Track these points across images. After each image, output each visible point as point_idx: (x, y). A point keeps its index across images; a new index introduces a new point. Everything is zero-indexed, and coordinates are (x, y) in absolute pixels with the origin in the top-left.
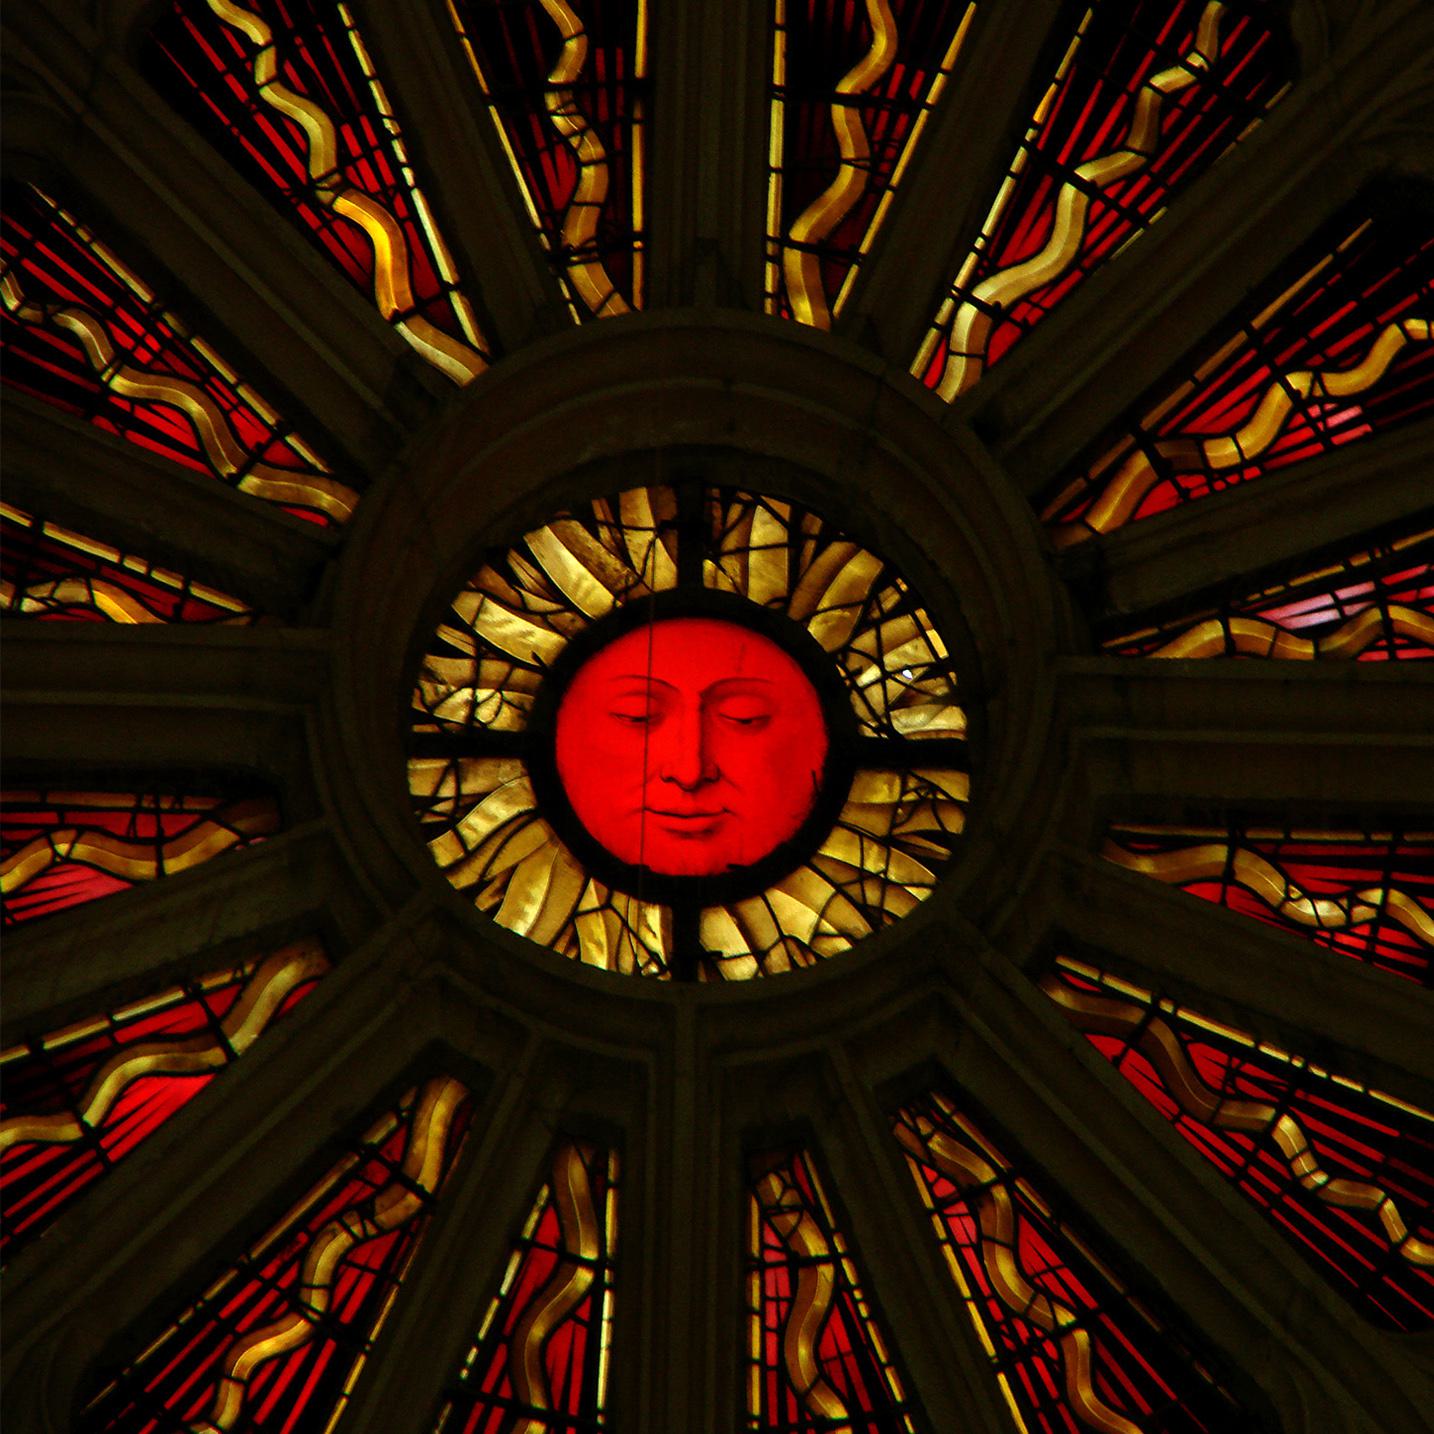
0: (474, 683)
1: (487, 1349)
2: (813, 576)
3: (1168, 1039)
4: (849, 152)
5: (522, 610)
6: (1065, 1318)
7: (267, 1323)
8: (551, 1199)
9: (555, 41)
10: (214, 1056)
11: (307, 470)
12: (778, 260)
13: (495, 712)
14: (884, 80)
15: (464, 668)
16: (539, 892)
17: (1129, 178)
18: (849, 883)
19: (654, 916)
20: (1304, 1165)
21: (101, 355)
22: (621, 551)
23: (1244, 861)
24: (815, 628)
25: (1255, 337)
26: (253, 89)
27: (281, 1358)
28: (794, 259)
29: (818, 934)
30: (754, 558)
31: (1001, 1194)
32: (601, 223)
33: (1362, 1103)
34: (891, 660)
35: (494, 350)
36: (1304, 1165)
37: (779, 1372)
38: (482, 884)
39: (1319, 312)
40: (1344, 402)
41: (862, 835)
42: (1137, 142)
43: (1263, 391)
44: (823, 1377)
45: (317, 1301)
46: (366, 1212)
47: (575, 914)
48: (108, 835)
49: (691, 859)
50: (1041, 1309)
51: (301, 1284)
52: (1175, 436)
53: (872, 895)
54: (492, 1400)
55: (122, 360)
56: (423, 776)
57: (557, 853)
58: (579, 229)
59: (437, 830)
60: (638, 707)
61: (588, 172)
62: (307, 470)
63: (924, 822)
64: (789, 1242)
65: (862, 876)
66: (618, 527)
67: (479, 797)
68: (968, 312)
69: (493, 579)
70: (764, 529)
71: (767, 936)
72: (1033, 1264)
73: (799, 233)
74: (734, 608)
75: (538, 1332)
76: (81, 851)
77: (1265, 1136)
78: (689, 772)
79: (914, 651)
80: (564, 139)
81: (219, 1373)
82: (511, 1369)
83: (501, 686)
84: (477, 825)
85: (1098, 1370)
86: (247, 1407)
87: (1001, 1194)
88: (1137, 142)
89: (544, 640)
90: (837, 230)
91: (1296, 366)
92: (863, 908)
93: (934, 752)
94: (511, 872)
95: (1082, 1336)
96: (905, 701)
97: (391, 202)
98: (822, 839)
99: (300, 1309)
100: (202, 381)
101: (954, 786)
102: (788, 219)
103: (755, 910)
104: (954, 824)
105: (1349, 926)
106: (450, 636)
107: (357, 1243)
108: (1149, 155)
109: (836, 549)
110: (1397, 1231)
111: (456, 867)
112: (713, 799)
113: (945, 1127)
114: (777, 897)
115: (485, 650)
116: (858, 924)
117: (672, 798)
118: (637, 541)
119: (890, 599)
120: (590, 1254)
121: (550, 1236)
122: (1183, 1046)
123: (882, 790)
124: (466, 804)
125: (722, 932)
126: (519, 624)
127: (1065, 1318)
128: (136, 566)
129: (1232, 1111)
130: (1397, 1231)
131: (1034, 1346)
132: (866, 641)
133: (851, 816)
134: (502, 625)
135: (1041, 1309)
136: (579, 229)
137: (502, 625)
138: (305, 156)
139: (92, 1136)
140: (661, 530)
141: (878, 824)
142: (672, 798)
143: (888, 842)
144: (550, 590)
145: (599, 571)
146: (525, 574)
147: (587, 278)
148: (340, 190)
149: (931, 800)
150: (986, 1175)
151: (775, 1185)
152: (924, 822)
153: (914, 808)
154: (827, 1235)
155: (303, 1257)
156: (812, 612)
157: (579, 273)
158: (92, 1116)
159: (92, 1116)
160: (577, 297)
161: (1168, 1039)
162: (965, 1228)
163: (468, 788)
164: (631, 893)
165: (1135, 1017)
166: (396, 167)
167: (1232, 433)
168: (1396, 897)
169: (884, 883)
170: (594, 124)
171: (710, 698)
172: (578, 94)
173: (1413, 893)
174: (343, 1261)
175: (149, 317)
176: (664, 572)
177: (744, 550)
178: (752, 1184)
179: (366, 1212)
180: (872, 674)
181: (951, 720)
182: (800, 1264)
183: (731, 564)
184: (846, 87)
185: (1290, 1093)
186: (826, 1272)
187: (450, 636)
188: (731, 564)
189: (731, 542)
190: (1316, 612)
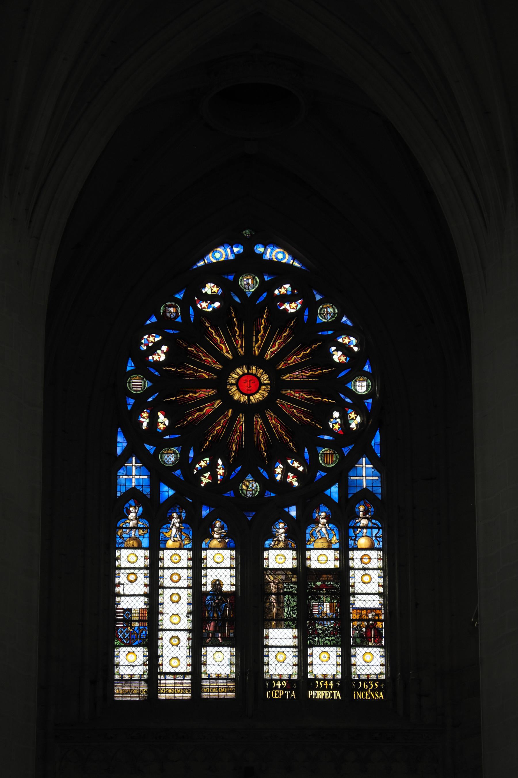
0: (232, 380)
1: (235, 428)
2: (258, 371)
3: (286, 405)
4: (260, 340)
5: (235, 374)
6: (278, 424)
7: (218, 426)
8: (239, 417)
9: (236, 332)
10: (213, 407)
11: (218, 364)
12: (254, 348)
13: (234, 382)
14: (262, 334)
15: (231, 379)
16: (237, 395)
17: (282, 342)
18: (261, 394)
19: (246, 397)
20: (296, 413)
21: (202, 356)
22: (243, 370)
23: (291, 391)
24: (258, 375)
25: (292, 353)
26: (213, 336)
27: (219, 429)
28: (256, 348)
29: (259, 398)
30: (253, 370)
31: (273, 416)
32: (241, 345)
33: (300, 409)
34: (264, 377)
35: (233, 356)
36: (296, 413)
37: (257, 429)
38: (233, 395)
39: (297, 351)
40: (299, 358)
41: (262, 390)
42: (282, 339)
43: (292, 357)
44: (260, 429)
45: (222, 425)
46: (225, 418)
47: (240, 397)
48: (204, 391)
49: (249, 392)
50: (276, 424)
51: (220, 423)
52: (286, 361)
53: (263, 395)
54: (235, 432)
55: (204, 356)
56: (228, 387)
57: (239, 392)
58: (239, 346)
59: (229, 391)
60: (245, 381)
61: (239, 342)
62: (218, 364)
63: (267, 389)
64: (257, 420)
65: (262, 393)
66: (243, 368)
67: (232, 388)
68: (269, 352)
69: (233, 372)
70: (254, 368)
71: (255, 398)
72: (276, 421)
73: (256, 346)
74: (252, 374)
75: (238, 426)
76: (202, 393)
77: (293, 411)
78: (249, 386)
79: (266, 377)
80: (237, 339)
81: (215, 430)
82: (236, 429)
83: (234, 380)
84: (232, 390)
85: (281, 428)
86: (217, 432)
87: (273, 416)
88: (282, 339)
89: (237, 377)
90: (259, 346)
91: (295, 355)
92: (262, 396)
93: (267, 384)
94: (235, 394)
95: (279, 426)
96: (265, 380)
97: (224, 344)
98: (259, 391)
99: (221, 425)
100: (210, 358)
101: (269, 387)
102: (255, 345)
103: (254, 396)
104: (269, 389)
105: (299, 396)
106: (230, 376)
107: (225, 420)
108: (283, 340)
109: (259, 369)
110: (303, 418)
111: (231, 393)
112: (250, 388)
113: (269, 411)
114: (256, 395)
115: (233, 377)
116: (262, 397)
117: (247, 388)
118: (244, 369)
119: (264, 373)
120: (242, 421)
121: (239, 420)
122: (287, 405)
123: (263, 387)
124: (232, 389)
125: (251, 398)
126: (235, 375)
127: (278, 424)
128: (206, 372)
129: (291, 410)
130: (303, 418)
131: (276, 427)
132: (262, 376)
133: (261, 389)
134: (234, 375)
135: (276, 424)
136: (239, 346)
137: (234, 375)
138: (217, 341)
139: (204, 413)
140: (246, 368)
141: (263, 390)
142: (247, 388)
143: (264, 391)
144: (238, 373)
145: (241, 371)
146: (235, 372)
147: (240, 350)
148: (220, 343)
149: (267, 388)
150: (272, 414)
151: (256, 416)
152: (267, 389)
153: (266, 388)
154: (260, 419)
155: (221, 421)
156: (258, 374)
157: (239, 349)
158: (204, 412)
159: (204, 412)
160: (239, 351)
161: (286, 405)
162: (270, 418)
163: (232, 387)
164: (245, 395)
165: (283, 403)
166: (224, 342)
167: (290, 360)
168: (303, 394)
169: (264, 394)
170: (240, 338)
171: (250, 381)
172: (238, 336)
173: (304, 394)
174: (223, 422)
175: (206, 353)
176: (246, 371)
177: (252, 370)
178: (254, 416)
179: (225, 418)
180: (262, 379)
181: (269, 382)
182: (258, 421)
183: (251, 371)
184: (259, 335)
185: (295, 408)
186: (260, 422)
187: (230, 376)
188: (251, 371)
189: (251, 369)
190: (297, 373)
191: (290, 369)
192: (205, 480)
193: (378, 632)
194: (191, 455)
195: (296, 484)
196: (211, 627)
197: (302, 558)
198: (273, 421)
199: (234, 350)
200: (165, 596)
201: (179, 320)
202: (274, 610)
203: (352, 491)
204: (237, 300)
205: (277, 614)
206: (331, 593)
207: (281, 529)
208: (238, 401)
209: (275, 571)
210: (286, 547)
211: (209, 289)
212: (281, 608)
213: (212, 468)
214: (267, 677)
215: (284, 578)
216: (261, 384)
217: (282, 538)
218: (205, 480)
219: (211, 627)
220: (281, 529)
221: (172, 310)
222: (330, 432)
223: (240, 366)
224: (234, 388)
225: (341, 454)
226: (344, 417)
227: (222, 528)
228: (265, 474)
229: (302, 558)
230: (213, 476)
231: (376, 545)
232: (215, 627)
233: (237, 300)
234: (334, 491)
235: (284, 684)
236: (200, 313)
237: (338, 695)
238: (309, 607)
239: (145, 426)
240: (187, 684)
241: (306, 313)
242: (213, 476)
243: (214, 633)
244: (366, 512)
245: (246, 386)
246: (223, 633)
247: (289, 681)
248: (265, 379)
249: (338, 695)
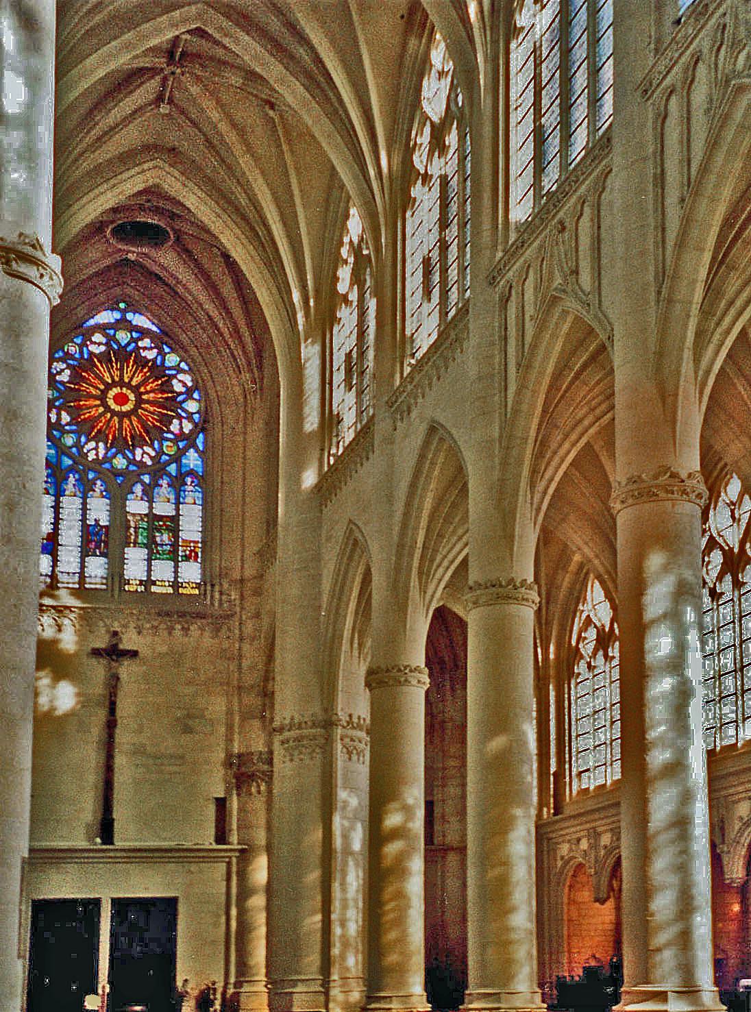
191: (147, 392)
192: (91, 456)
193: (196, 554)
194: (83, 439)
195: (149, 463)
196: (92, 546)
197: (151, 508)
198: (135, 424)
200: (63, 526)
201: (77, 356)
202: (133, 537)
203: (183, 470)
204: (115, 347)
205: (135, 540)
206: (168, 529)
207: (138, 489)
208: (114, 410)
209: (134, 515)
210: (142, 499)
211: (98, 337)
212: (137, 537)
213: (96, 448)
214: (126, 577)
215: (139, 518)
217: (140, 494)
218: (91, 456)
219: (92, 546)
220: (138, 489)
222: (172, 433)
223: (116, 387)
226: (181, 424)
227: (102, 485)
228: (130, 455)
229: (151, 508)
230: (97, 454)
231: (197, 502)
232: (95, 545)
233: (115, 347)
234: (172, 468)
235: (138, 582)
236: (90, 353)
237: (170, 590)
238: (154, 537)
240: (76, 578)
242: (97, 454)
243: (94, 550)
244: (192, 482)
246: (100, 549)
247: (141, 581)
248: (132, 397)
249: (170, 590)
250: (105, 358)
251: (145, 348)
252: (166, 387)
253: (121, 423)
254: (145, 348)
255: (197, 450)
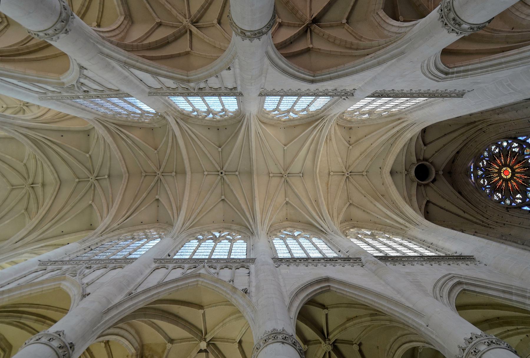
199: (497, 177)
208: (511, 176)
216: (506, 170)
221: (487, 191)
223: (501, 175)
224: (507, 176)
225: (526, 147)
226: (514, 148)
236: (488, 184)
239: (521, 201)
241: (486, 159)
245: (507, 174)
250: (489, 179)
251: (483, 164)
252: (499, 155)
253: (518, 173)
254: (483, 164)
255: (527, 139)
